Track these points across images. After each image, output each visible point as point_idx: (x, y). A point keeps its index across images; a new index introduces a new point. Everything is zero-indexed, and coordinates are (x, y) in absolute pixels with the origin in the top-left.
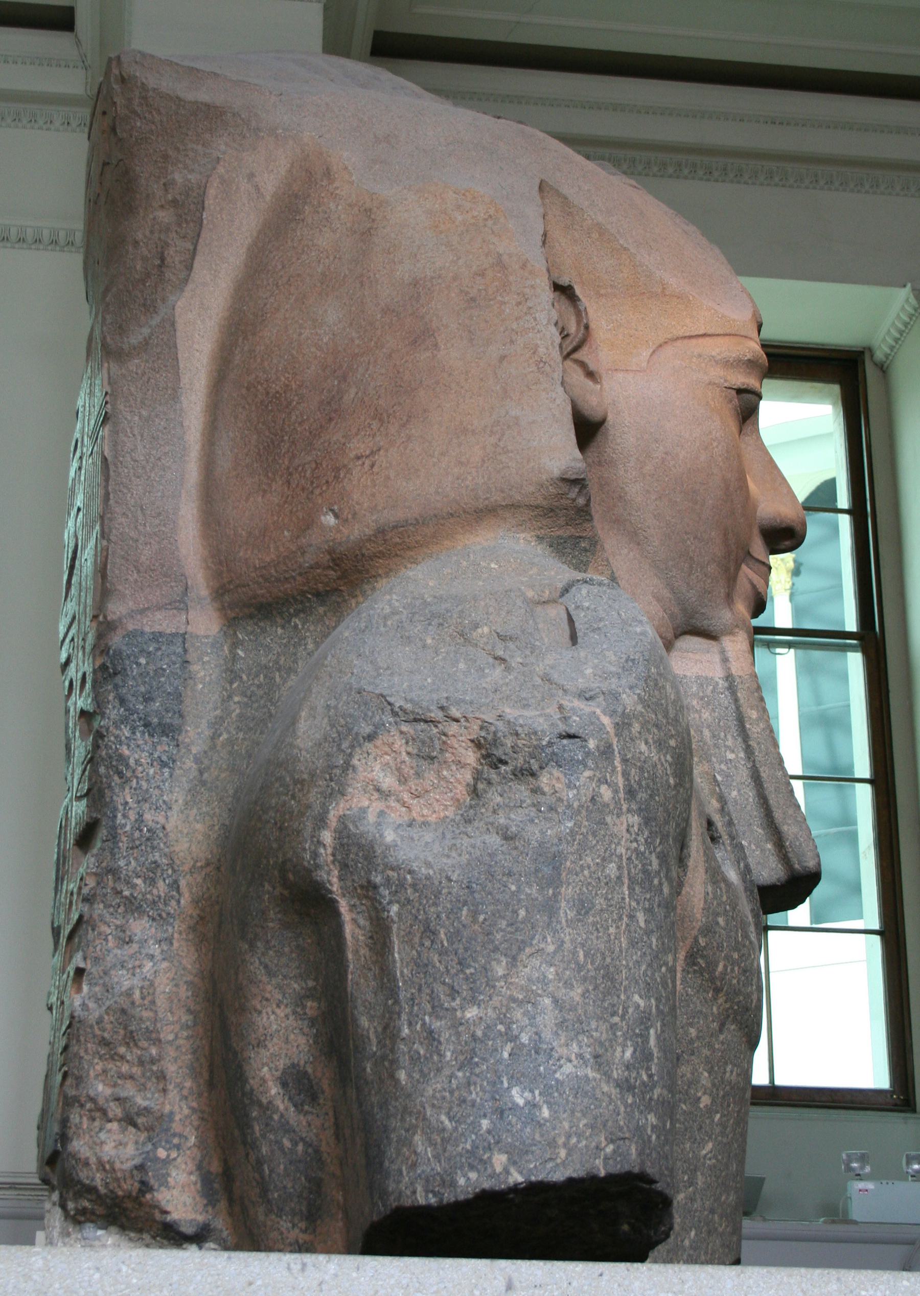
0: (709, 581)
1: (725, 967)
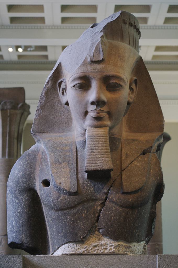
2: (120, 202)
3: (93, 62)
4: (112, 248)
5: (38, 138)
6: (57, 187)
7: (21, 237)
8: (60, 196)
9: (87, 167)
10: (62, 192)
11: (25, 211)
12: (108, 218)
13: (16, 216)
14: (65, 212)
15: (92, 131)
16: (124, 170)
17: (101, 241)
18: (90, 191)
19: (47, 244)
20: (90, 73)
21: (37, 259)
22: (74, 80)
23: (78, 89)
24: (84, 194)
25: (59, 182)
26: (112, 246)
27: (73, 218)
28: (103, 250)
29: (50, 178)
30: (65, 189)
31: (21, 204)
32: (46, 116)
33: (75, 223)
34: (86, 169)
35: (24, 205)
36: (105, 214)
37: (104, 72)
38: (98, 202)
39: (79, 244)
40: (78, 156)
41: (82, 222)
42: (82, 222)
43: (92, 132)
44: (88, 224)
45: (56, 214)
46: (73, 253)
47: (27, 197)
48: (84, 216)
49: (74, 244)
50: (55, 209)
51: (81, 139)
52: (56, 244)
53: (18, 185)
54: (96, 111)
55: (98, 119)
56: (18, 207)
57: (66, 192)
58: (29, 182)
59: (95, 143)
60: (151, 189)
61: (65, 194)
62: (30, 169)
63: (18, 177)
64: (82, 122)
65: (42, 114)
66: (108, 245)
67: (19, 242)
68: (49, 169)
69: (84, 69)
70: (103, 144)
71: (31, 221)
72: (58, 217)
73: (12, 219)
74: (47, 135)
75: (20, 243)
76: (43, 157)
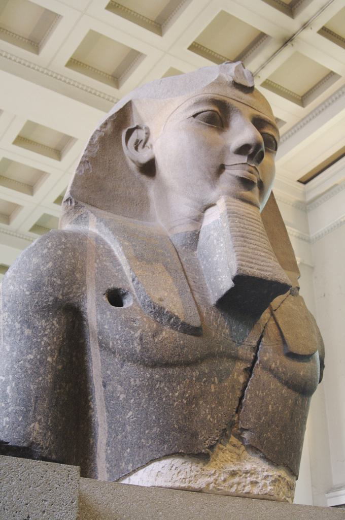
0: (200, 187)
1: (113, 343)
2: (283, 373)
4: (268, 482)
5: (83, 211)
6: (154, 308)
7: (28, 430)
8: (162, 331)
9: (242, 267)
10: (164, 321)
11: (49, 359)
12: (262, 406)
13: (19, 371)
14: (170, 371)
15: (236, 204)
16: (276, 310)
17: (244, 462)
18: (223, 335)
19: (88, 461)
20: (231, 99)
22: (198, 103)
23: (203, 122)
24: (214, 338)
25: (158, 297)
26: (266, 477)
27: (189, 391)
28: (249, 486)
30: (175, 316)
31: (39, 340)
32: (99, 178)
33: (194, 406)
34: (242, 272)
35: (48, 344)
36: (256, 395)
37: (255, 109)
38: (239, 363)
39: (198, 463)
40: (182, 261)
41: (208, 406)
42: (208, 406)
43: (237, 206)
44: (222, 413)
45: (145, 373)
46: (183, 485)
47: (57, 326)
48: (213, 391)
49: (185, 463)
50: (146, 360)
52: (129, 460)
53: (36, 292)
54: (247, 168)
56: (31, 348)
57: (175, 323)
58: (69, 289)
59: (247, 227)
61: (172, 328)
62: (73, 261)
63: (39, 272)
64: (207, 186)
65: (91, 172)
67: (20, 442)
68: (121, 270)
70: (262, 234)
71: (60, 389)
72: (149, 385)
73: (4, 379)
74: (102, 212)
75: (25, 445)
76: (99, 246)
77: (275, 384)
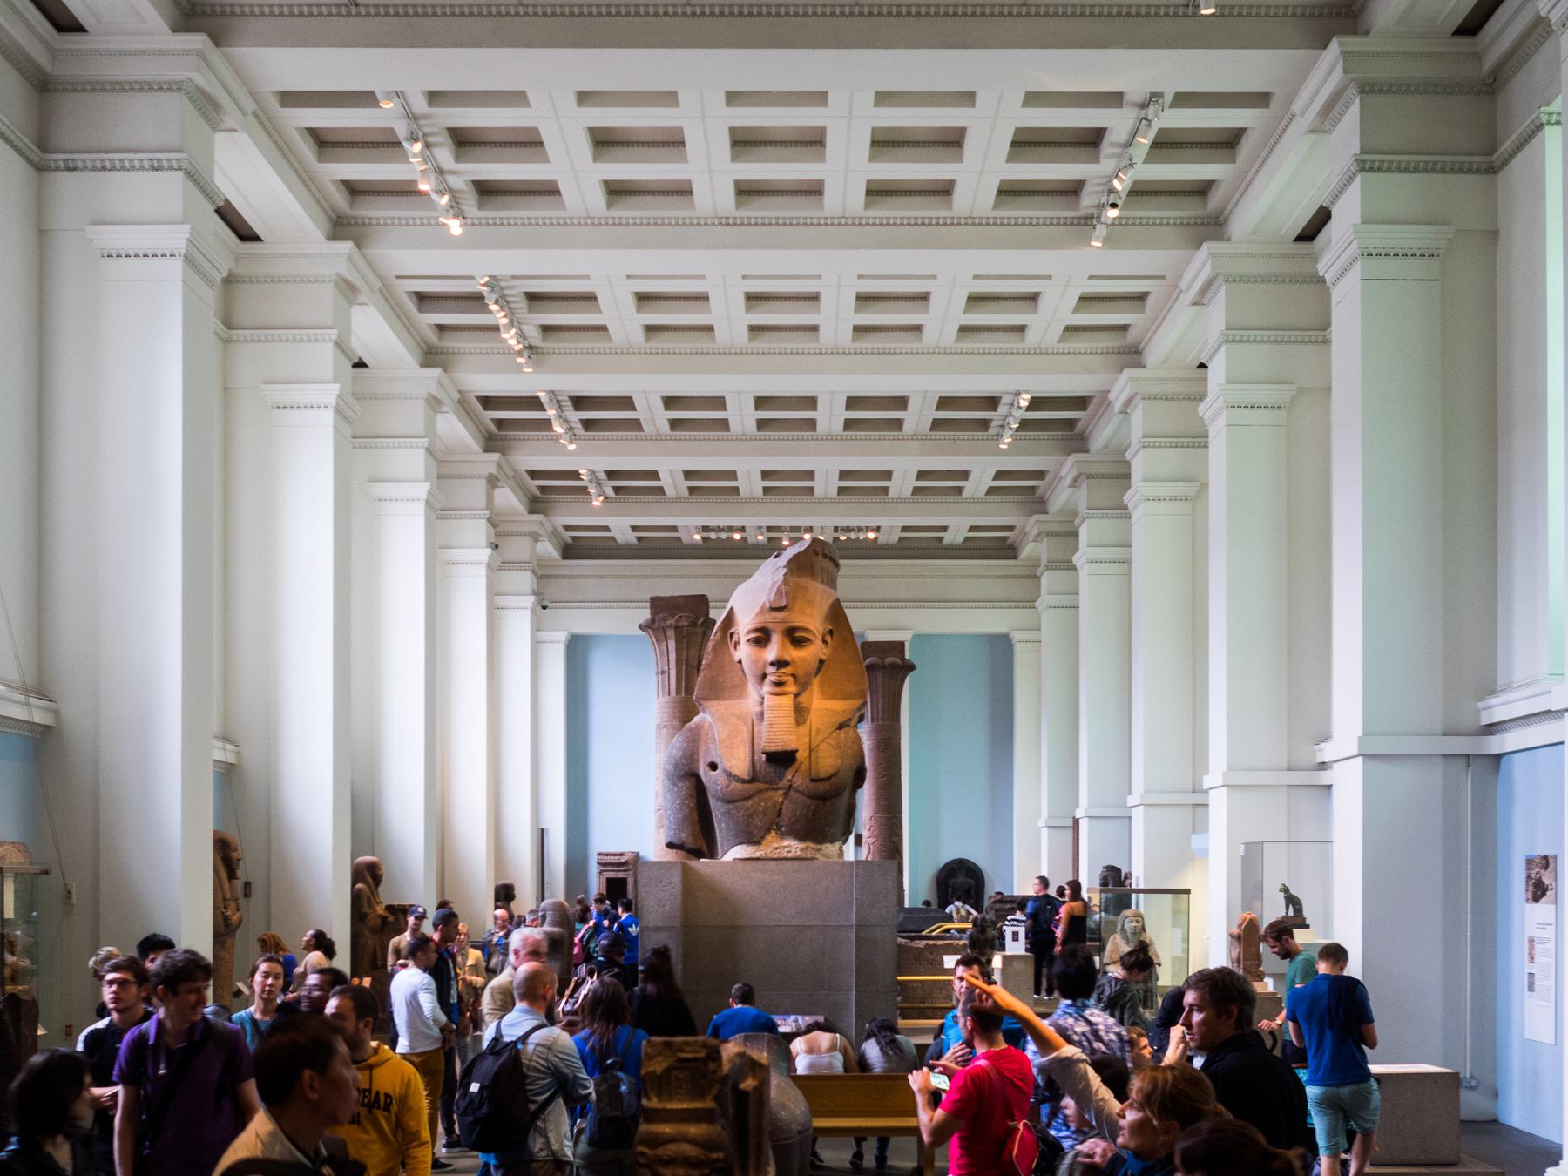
3: (773, 609)
21: (702, 865)
22: (749, 632)
29: (717, 760)
51: (758, 709)
55: (779, 684)
60: (849, 776)
66: (792, 846)
69: (761, 619)
77: (801, 798)
